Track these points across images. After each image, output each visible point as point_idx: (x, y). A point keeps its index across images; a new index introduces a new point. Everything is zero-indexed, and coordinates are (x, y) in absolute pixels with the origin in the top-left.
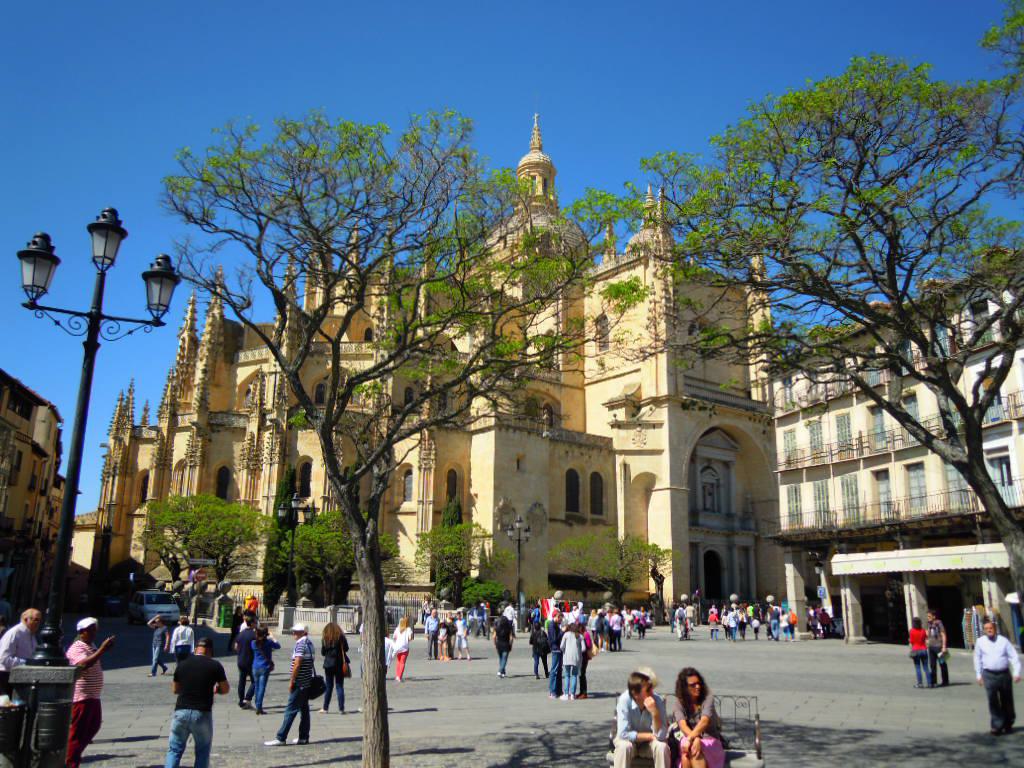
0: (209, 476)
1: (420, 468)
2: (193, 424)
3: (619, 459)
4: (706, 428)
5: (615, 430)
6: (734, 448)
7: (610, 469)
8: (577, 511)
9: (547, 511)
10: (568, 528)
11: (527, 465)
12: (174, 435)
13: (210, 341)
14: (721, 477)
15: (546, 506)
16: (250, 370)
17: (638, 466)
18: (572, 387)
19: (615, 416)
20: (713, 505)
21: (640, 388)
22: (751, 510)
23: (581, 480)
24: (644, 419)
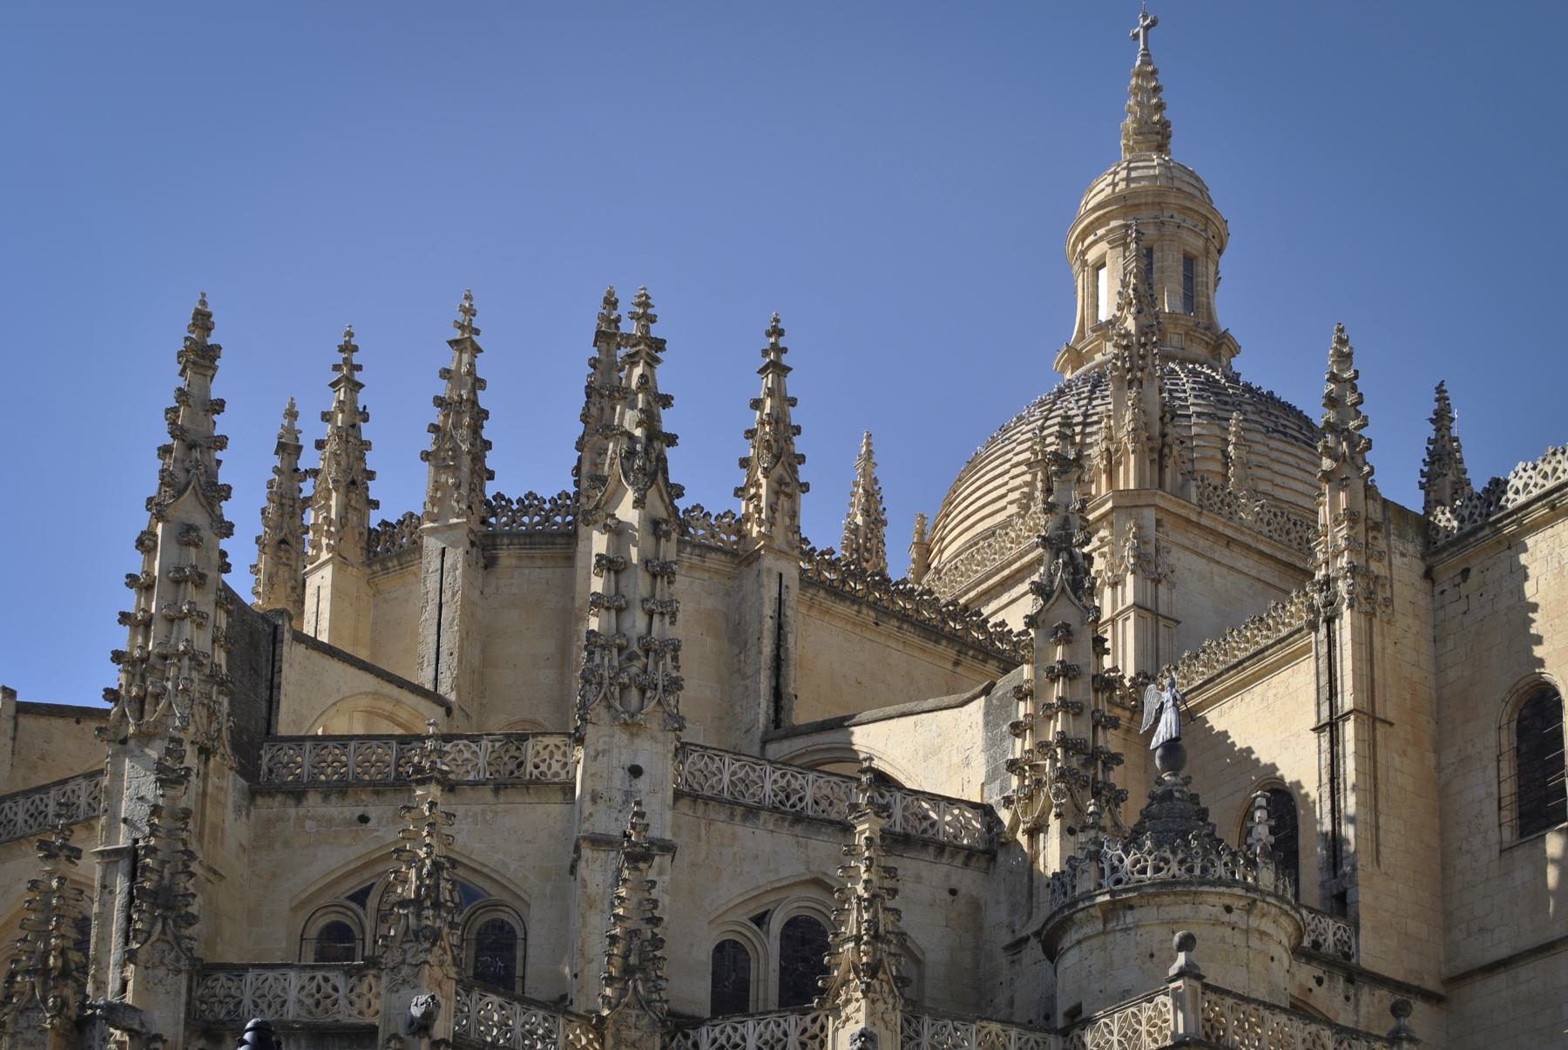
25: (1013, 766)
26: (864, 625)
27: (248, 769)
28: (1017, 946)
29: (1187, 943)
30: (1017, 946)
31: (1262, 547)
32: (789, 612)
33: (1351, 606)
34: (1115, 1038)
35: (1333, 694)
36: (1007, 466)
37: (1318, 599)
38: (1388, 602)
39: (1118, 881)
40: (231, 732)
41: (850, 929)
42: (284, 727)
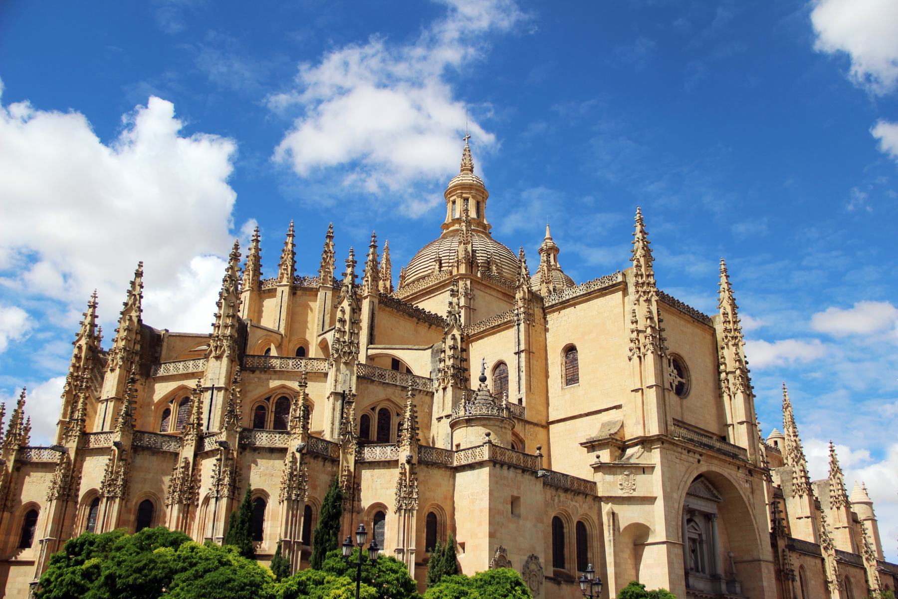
0: (129, 511)
1: (399, 509)
2: (116, 444)
3: (606, 508)
4: (695, 474)
5: (600, 474)
6: (714, 499)
7: (595, 518)
8: (563, 568)
9: (543, 565)
10: (556, 587)
11: (523, 510)
12: (83, 461)
13: (125, 349)
14: (703, 533)
15: (542, 560)
16: (172, 386)
17: (628, 515)
18: (536, 425)
19: (598, 457)
20: (696, 562)
21: (622, 426)
22: (734, 571)
23: (565, 530)
24: (632, 461)
25: (439, 371)
26: (393, 314)
27: (241, 365)
28: (439, 419)
29: (488, 435)
30: (439, 419)
31: (498, 289)
32: (375, 312)
33: (524, 322)
34: (470, 455)
35: (519, 344)
36: (428, 259)
37: (516, 318)
38: (534, 321)
39: (470, 413)
40: (229, 346)
41: (405, 426)
42: (249, 351)
